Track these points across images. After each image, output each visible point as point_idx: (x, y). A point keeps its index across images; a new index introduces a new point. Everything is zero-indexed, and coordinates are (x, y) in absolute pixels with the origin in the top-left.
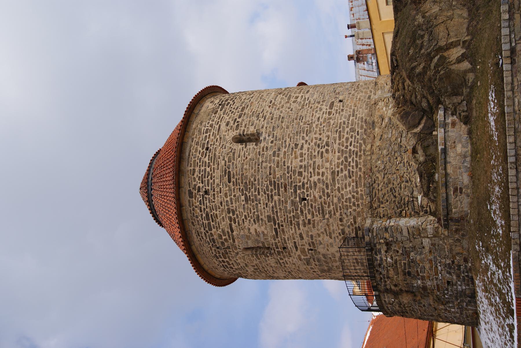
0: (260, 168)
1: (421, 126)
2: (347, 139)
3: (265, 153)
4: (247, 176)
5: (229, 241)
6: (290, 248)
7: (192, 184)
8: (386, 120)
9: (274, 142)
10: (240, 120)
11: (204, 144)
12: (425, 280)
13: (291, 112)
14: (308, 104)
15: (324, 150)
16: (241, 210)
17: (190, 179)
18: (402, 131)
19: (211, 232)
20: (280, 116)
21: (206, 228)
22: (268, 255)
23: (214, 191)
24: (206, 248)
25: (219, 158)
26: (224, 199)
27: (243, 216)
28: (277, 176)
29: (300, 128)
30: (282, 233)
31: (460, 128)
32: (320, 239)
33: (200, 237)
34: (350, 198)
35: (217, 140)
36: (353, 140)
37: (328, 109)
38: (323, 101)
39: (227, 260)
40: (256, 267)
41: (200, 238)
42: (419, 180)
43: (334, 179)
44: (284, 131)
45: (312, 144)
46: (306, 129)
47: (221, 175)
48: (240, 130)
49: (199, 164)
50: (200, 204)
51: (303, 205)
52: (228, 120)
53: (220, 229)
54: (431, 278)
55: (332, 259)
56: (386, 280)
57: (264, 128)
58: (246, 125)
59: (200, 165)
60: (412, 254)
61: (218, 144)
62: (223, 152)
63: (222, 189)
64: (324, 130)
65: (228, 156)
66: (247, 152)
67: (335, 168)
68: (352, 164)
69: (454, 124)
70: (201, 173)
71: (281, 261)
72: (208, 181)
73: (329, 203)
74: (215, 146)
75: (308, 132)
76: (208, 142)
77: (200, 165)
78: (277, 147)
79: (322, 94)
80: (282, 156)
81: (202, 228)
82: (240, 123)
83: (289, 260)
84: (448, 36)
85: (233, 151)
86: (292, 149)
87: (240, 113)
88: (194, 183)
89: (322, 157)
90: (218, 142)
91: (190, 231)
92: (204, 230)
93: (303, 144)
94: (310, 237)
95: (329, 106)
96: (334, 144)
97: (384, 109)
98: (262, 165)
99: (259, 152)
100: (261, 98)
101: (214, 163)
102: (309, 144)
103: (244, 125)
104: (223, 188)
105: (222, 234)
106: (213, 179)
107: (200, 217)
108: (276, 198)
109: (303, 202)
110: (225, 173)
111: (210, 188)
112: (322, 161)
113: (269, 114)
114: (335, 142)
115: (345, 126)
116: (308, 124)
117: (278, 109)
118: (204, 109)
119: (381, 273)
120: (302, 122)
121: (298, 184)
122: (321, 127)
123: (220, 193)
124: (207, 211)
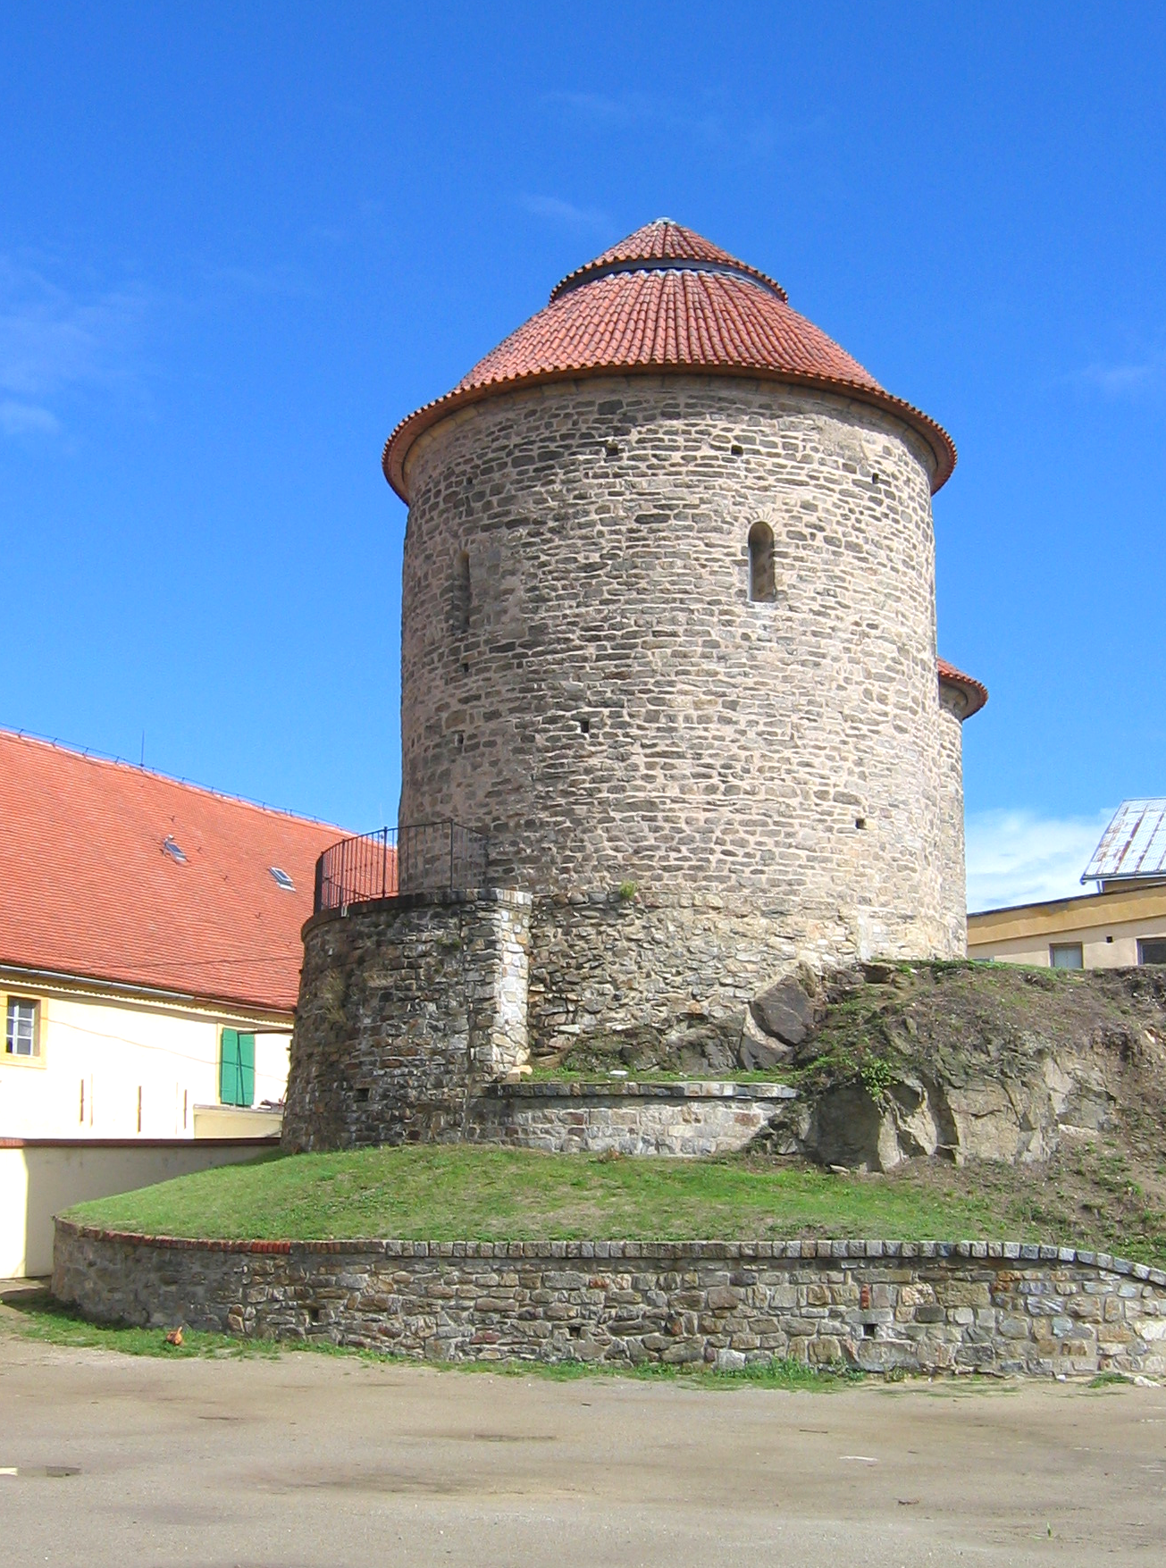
0: (674, 605)
1: (760, 1037)
2: (742, 843)
3: (715, 619)
4: (653, 569)
5: (485, 516)
6: (466, 684)
7: (638, 410)
8: (788, 948)
9: (746, 644)
10: (819, 541)
11: (752, 441)
12: (371, 1036)
13: (834, 685)
14: (856, 732)
15: (715, 780)
16: (564, 553)
17: (653, 403)
18: (751, 989)
19: (510, 464)
20: (824, 656)
21: (520, 451)
22: (451, 622)
23: (616, 476)
24: (469, 448)
25: (706, 488)
26: (592, 503)
27: (548, 558)
28: (649, 653)
29: (781, 715)
30: (502, 663)
31: (735, 1136)
32: (486, 767)
33: (497, 434)
34: (582, 849)
35: (759, 478)
36: (739, 859)
37: (837, 789)
38: (863, 776)
39: (442, 506)
40: (423, 584)
41: (493, 433)
42: (619, 1028)
43: (633, 806)
44: (777, 669)
45: (734, 749)
46: (779, 731)
47: (659, 494)
48: (788, 545)
49: (693, 429)
50: (583, 436)
51: (572, 722)
52: (820, 508)
53: (517, 490)
54: (376, 1050)
55: (439, 795)
56: (375, 938)
57: (790, 614)
58: (801, 559)
59: (689, 433)
60: (432, 1007)
61: (748, 482)
62: (725, 497)
63: (620, 498)
64: (772, 779)
65: (712, 513)
66: (720, 567)
67: (664, 811)
68: (673, 855)
69: (746, 1120)
70: (666, 437)
71: (435, 656)
72: (643, 459)
73: (573, 794)
74: (742, 473)
75: (768, 738)
76: (757, 452)
77: (689, 433)
78: (731, 650)
79: (888, 769)
80: (705, 667)
81: (517, 440)
82: (810, 542)
83: (438, 677)
84: (973, 1115)
85: (725, 526)
86: (724, 695)
87: (843, 539)
88: (640, 416)
89: (697, 776)
90: (755, 481)
91: (514, 404)
92: (515, 446)
93: (736, 723)
94: (492, 739)
95: (846, 791)
96: (730, 808)
97: (824, 942)
98: (682, 610)
99: (719, 602)
100: (887, 596)
101: (694, 473)
102: (732, 741)
103: (802, 553)
104: (624, 500)
105: (502, 496)
106: (650, 472)
107: (547, 434)
108: (591, 650)
109: (578, 723)
110: (662, 507)
111: (625, 463)
112: (684, 777)
113: (832, 624)
114: (737, 811)
115: (781, 838)
116: (792, 735)
117: (847, 650)
118: (864, 433)
119: (389, 926)
120: (802, 718)
121: (625, 712)
122: (783, 771)
123: (610, 494)
124: (561, 455)
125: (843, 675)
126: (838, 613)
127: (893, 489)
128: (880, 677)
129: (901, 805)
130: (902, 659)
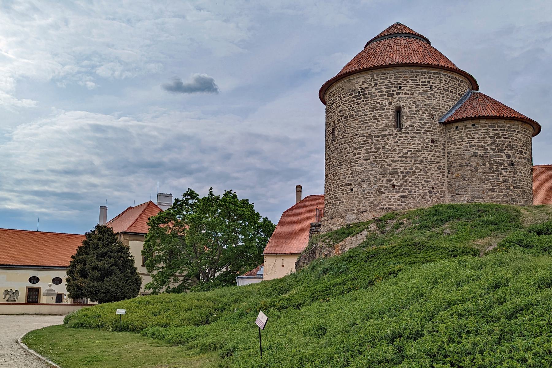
10: (343, 119)
13: (345, 156)
20: (343, 149)
38: (353, 177)
48: (337, 124)
79: (361, 172)
87: (348, 115)
125: (347, 152)
126: (347, 136)
127: (366, 92)
128: (358, 148)
129: (365, 181)
130: (368, 139)
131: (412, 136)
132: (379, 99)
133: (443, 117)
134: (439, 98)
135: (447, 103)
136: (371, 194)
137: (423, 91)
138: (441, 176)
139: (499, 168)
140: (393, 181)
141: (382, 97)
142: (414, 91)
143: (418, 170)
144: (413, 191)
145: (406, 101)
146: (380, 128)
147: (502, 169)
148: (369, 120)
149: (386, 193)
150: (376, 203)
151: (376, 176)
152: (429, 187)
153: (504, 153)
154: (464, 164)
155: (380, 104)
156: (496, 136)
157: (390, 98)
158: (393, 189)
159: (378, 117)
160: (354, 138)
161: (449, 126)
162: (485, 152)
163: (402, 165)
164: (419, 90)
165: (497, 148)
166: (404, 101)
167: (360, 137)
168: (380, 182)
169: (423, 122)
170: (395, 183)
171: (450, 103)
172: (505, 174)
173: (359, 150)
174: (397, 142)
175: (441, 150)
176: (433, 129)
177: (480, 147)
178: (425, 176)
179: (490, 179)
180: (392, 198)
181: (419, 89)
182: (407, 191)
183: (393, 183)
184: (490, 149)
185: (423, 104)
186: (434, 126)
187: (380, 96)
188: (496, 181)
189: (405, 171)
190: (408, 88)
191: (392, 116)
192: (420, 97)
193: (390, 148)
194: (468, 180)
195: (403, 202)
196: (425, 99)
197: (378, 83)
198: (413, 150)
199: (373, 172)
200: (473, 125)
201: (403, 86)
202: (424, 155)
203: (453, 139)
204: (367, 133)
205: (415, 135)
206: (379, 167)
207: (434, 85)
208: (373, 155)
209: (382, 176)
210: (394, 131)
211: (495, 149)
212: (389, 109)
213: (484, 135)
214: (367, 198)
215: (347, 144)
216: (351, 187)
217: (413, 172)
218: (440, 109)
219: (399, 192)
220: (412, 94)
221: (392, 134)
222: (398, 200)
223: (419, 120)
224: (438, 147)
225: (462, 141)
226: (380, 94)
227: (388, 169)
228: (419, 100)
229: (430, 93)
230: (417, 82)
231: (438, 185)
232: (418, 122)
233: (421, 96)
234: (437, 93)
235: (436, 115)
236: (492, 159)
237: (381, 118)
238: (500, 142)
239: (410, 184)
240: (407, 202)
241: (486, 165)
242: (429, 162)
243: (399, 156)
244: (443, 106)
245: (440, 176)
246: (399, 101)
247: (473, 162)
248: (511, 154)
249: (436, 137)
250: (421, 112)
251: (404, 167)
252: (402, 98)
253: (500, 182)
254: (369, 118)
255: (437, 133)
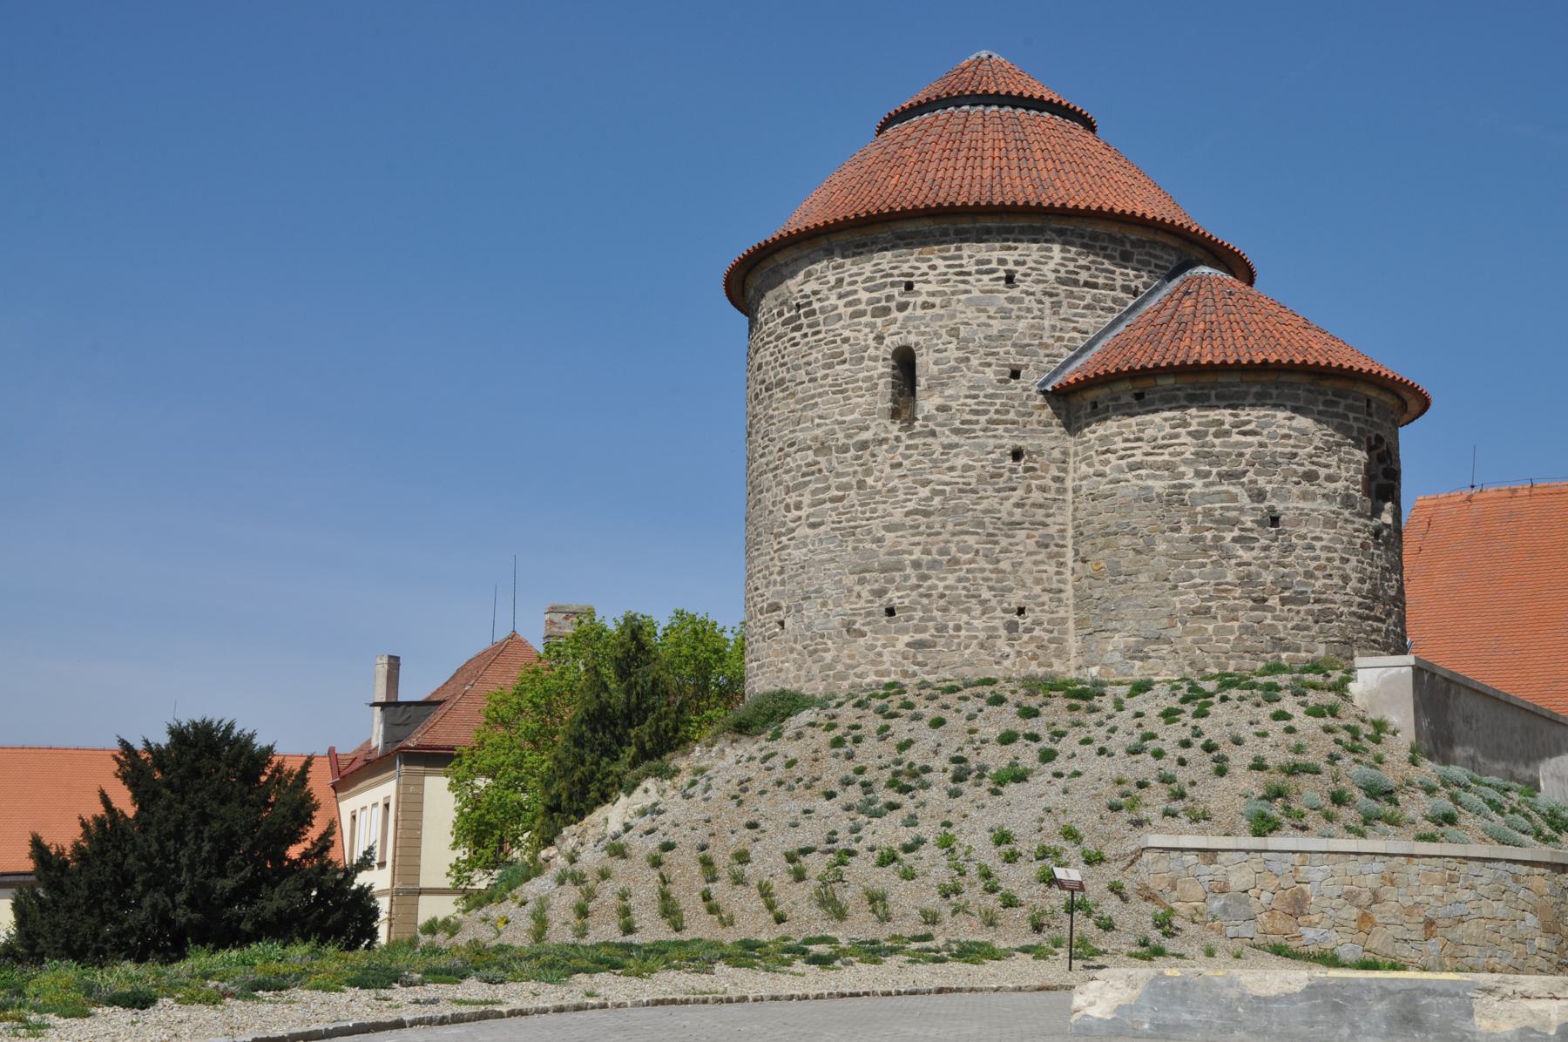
13: (767, 512)
38: (783, 583)
129: (813, 595)
130: (819, 459)
131: (946, 441)
132: (849, 325)
133: (1055, 373)
134: (1040, 310)
135: (1072, 325)
136: (825, 640)
137: (982, 292)
138: (1052, 569)
139: (1224, 538)
140: (889, 595)
141: (856, 320)
142: (953, 293)
143: (968, 553)
144: (951, 625)
145: (927, 329)
146: (852, 422)
147: (1234, 540)
148: (820, 395)
149: (869, 634)
150: (840, 667)
151: (841, 580)
152: (1005, 611)
153: (1243, 484)
154: (1114, 529)
155: (852, 341)
156: (1212, 430)
157: (879, 321)
158: (888, 621)
159: (844, 386)
160: (788, 455)
161: (1074, 400)
162: (1174, 486)
163: (917, 539)
164: (966, 292)
165: (1215, 470)
166: (922, 329)
167: (799, 450)
168: (853, 599)
169: (982, 394)
170: (896, 601)
171: (1089, 322)
172: (1246, 556)
173: (797, 493)
174: (899, 465)
175: (1052, 484)
176: (1019, 414)
177: (1159, 468)
178: (992, 571)
179: (1192, 577)
180: (886, 652)
181: (968, 287)
182: (931, 624)
183: (890, 600)
184: (1192, 474)
185: (982, 336)
186: (1020, 406)
187: (854, 315)
188: (1212, 582)
189: (926, 558)
190: (933, 287)
191: (883, 380)
192: (971, 313)
193: (880, 484)
194: (1125, 582)
195: (919, 664)
196: (989, 317)
197: (846, 275)
198: (948, 488)
199: (833, 565)
200: (1139, 396)
201: (917, 282)
202: (985, 504)
203: (1086, 442)
204: (815, 439)
205: (955, 439)
206: (849, 548)
207: (1021, 269)
208: (833, 509)
209: (856, 577)
210: (891, 427)
211: (1208, 474)
212: (875, 359)
213: (1173, 427)
214: (816, 651)
215: (770, 475)
216: (779, 616)
217: (949, 561)
218: (1043, 345)
219: (905, 631)
220: (944, 304)
221: (885, 441)
222: (905, 658)
223: (971, 388)
224: (1039, 473)
225: (1108, 451)
226: (850, 310)
227: (874, 554)
228: (967, 324)
229: (1006, 295)
230: (961, 266)
231: (1041, 600)
232: (966, 397)
233: (973, 309)
234: (1032, 294)
235: (1027, 366)
236: (1199, 509)
237: (853, 389)
238: (1225, 446)
239: (942, 602)
240: (932, 664)
241: (1178, 530)
242: (1004, 524)
243: (906, 509)
244: (1057, 334)
245: (1045, 571)
246: (904, 331)
247: (1140, 519)
248: (1269, 488)
249: (1030, 441)
250: (974, 362)
251: (920, 548)
252: (915, 318)
253: (1227, 583)
254: (821, 390)
255: (1035, 426)
